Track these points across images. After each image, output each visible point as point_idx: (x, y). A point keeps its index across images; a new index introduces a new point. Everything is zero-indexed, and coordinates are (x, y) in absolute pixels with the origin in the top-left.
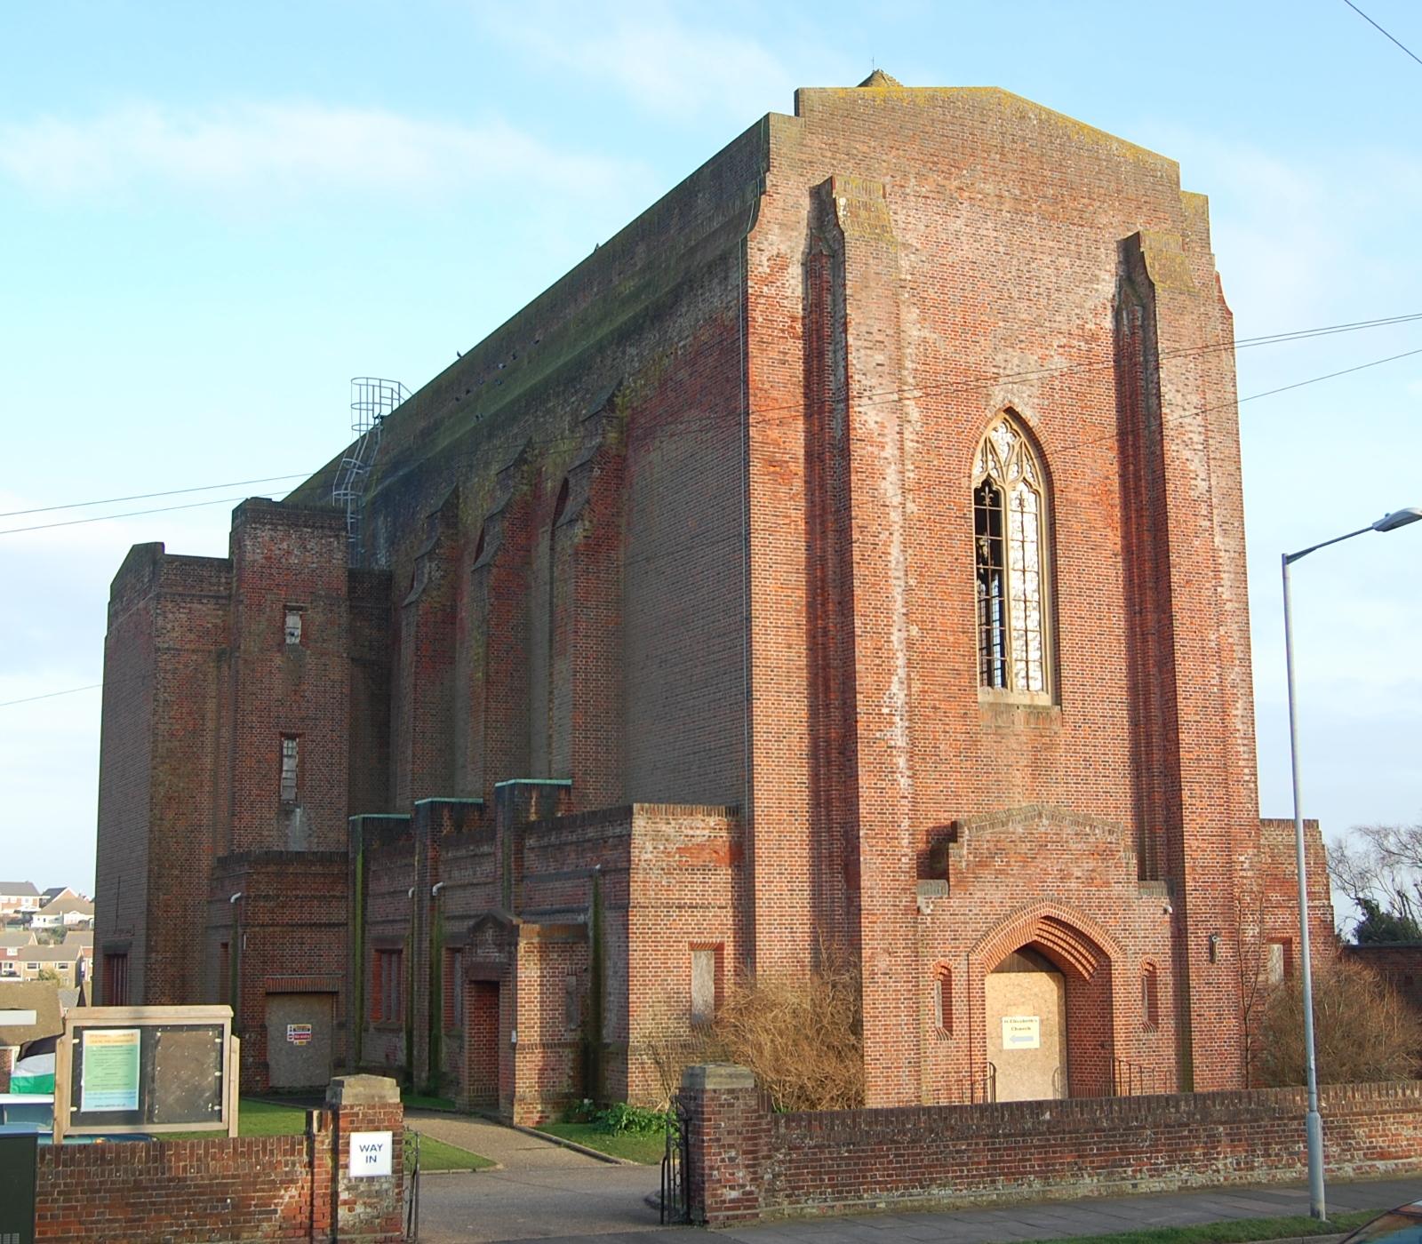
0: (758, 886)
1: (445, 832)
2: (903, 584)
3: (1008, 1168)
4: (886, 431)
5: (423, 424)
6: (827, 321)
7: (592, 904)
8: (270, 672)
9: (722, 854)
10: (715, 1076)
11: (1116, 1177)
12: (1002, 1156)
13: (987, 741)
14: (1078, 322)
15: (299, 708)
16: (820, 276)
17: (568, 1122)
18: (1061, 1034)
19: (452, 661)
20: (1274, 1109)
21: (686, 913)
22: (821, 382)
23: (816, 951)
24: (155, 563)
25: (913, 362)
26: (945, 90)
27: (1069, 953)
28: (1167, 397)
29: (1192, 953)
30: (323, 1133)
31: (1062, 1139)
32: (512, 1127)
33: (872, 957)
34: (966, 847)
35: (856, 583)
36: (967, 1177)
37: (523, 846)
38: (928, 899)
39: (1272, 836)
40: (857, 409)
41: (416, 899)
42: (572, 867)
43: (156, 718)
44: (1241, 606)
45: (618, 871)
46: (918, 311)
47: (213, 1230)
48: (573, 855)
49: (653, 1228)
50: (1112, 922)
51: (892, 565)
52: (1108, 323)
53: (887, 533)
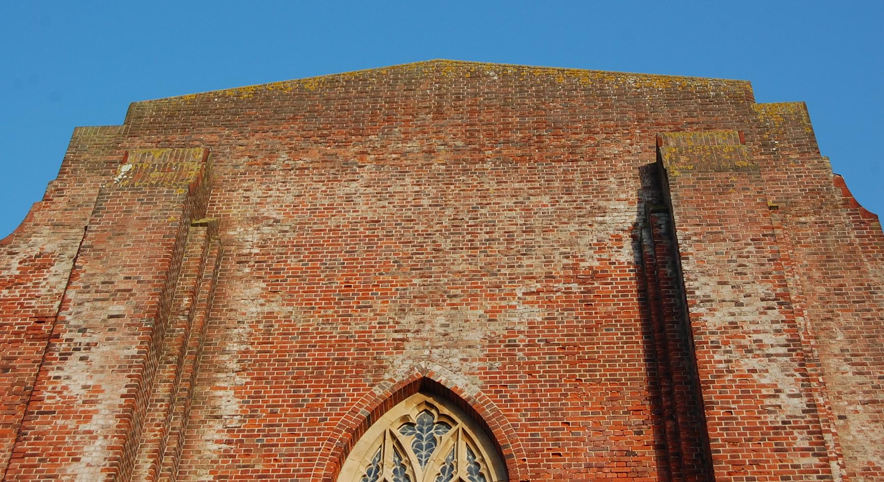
14: (565, 261)
28: (697, 293)
46: (264, 285)
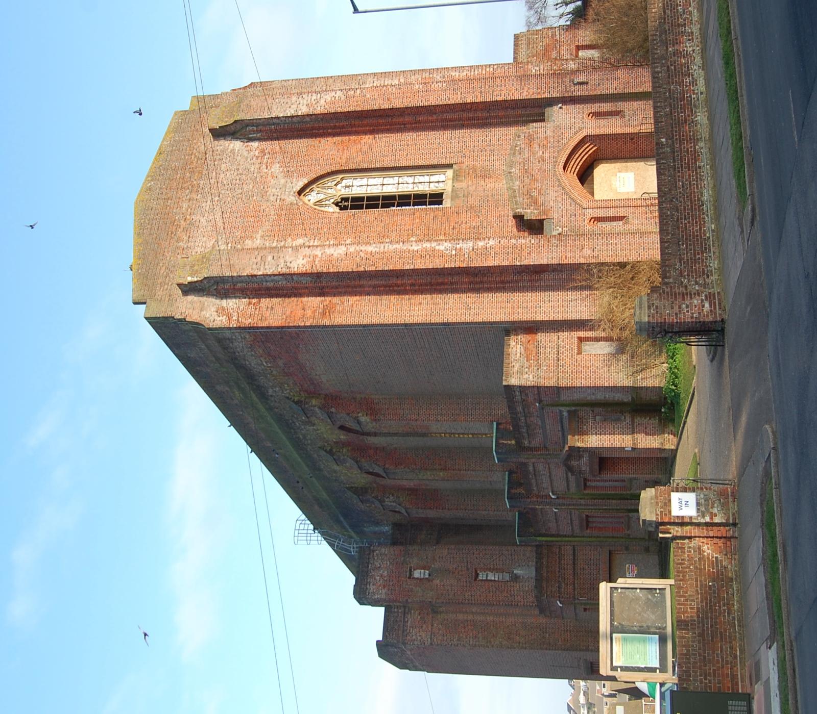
0: (547, 319)
1: (523, 492)
2: (387, 245)
3: (692, 159)
4: (308, 254)
5: (316, 507)
6: (251, 286)
7: (557, 408)
8: (443, 586)
9: (530, 338)
10: (641, 317)
11: (697, 103)
12: (685, 163)
13: (471, 201)
15: (462, 571)
16: (228, 289)
17: (674, 420)
18: (626, 162)
19: (436, 490)
20: (660, 22)
21: (561, 356)
22: (282, 288)
23: (582, 288)
24: (387, 645)
25: (273, 242)
26: (135, 228)
27: (583, 157)
28: (293, 113)
29: (583, 93)
30: (672, 531)
31: (676, 132)
32: (677, 450)
33: (584, 257)
34: (526, 210)
35: (386, 268)
36: (697, 181)
37: (529, 447)
38: (553, 229)
39: (522, 57)
40: (296, 269)
41: (559, 507)
42: (538, 419)
43: (467, 645)
44: (402, 74)
45: (539, 393)
46: (247, 240)
47: (727, 592)
48: (532, 419)
49: (727, 349)
50: (566, 135)
51: (377, 250)
52: (255, 144)
53: (361, 253)
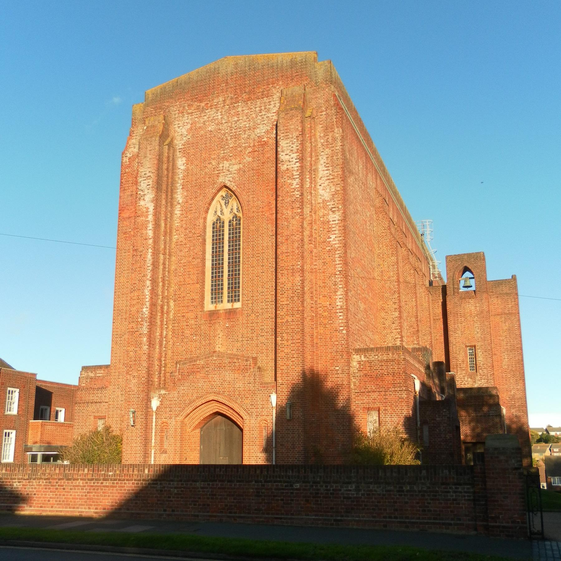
34: (178, 372)
